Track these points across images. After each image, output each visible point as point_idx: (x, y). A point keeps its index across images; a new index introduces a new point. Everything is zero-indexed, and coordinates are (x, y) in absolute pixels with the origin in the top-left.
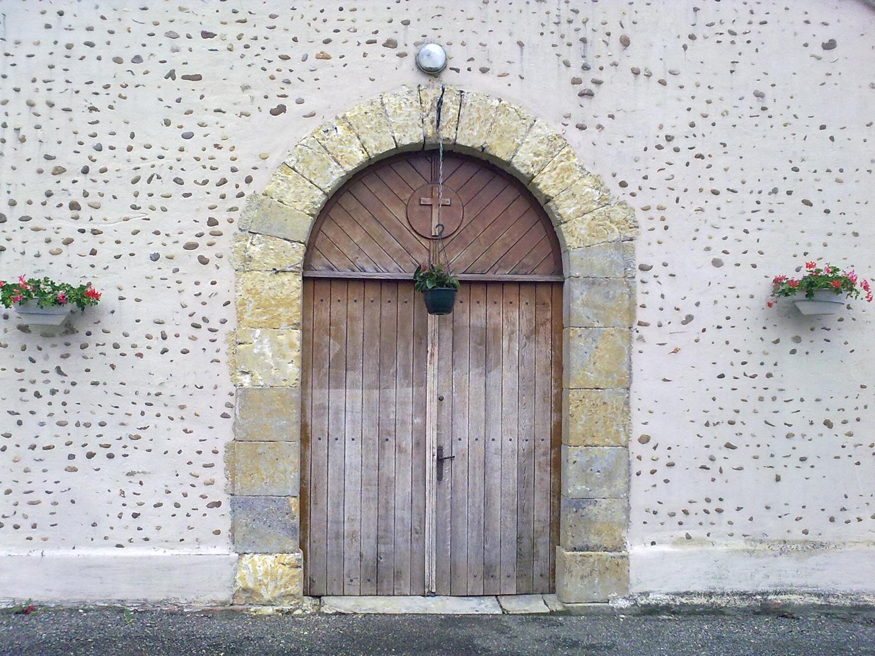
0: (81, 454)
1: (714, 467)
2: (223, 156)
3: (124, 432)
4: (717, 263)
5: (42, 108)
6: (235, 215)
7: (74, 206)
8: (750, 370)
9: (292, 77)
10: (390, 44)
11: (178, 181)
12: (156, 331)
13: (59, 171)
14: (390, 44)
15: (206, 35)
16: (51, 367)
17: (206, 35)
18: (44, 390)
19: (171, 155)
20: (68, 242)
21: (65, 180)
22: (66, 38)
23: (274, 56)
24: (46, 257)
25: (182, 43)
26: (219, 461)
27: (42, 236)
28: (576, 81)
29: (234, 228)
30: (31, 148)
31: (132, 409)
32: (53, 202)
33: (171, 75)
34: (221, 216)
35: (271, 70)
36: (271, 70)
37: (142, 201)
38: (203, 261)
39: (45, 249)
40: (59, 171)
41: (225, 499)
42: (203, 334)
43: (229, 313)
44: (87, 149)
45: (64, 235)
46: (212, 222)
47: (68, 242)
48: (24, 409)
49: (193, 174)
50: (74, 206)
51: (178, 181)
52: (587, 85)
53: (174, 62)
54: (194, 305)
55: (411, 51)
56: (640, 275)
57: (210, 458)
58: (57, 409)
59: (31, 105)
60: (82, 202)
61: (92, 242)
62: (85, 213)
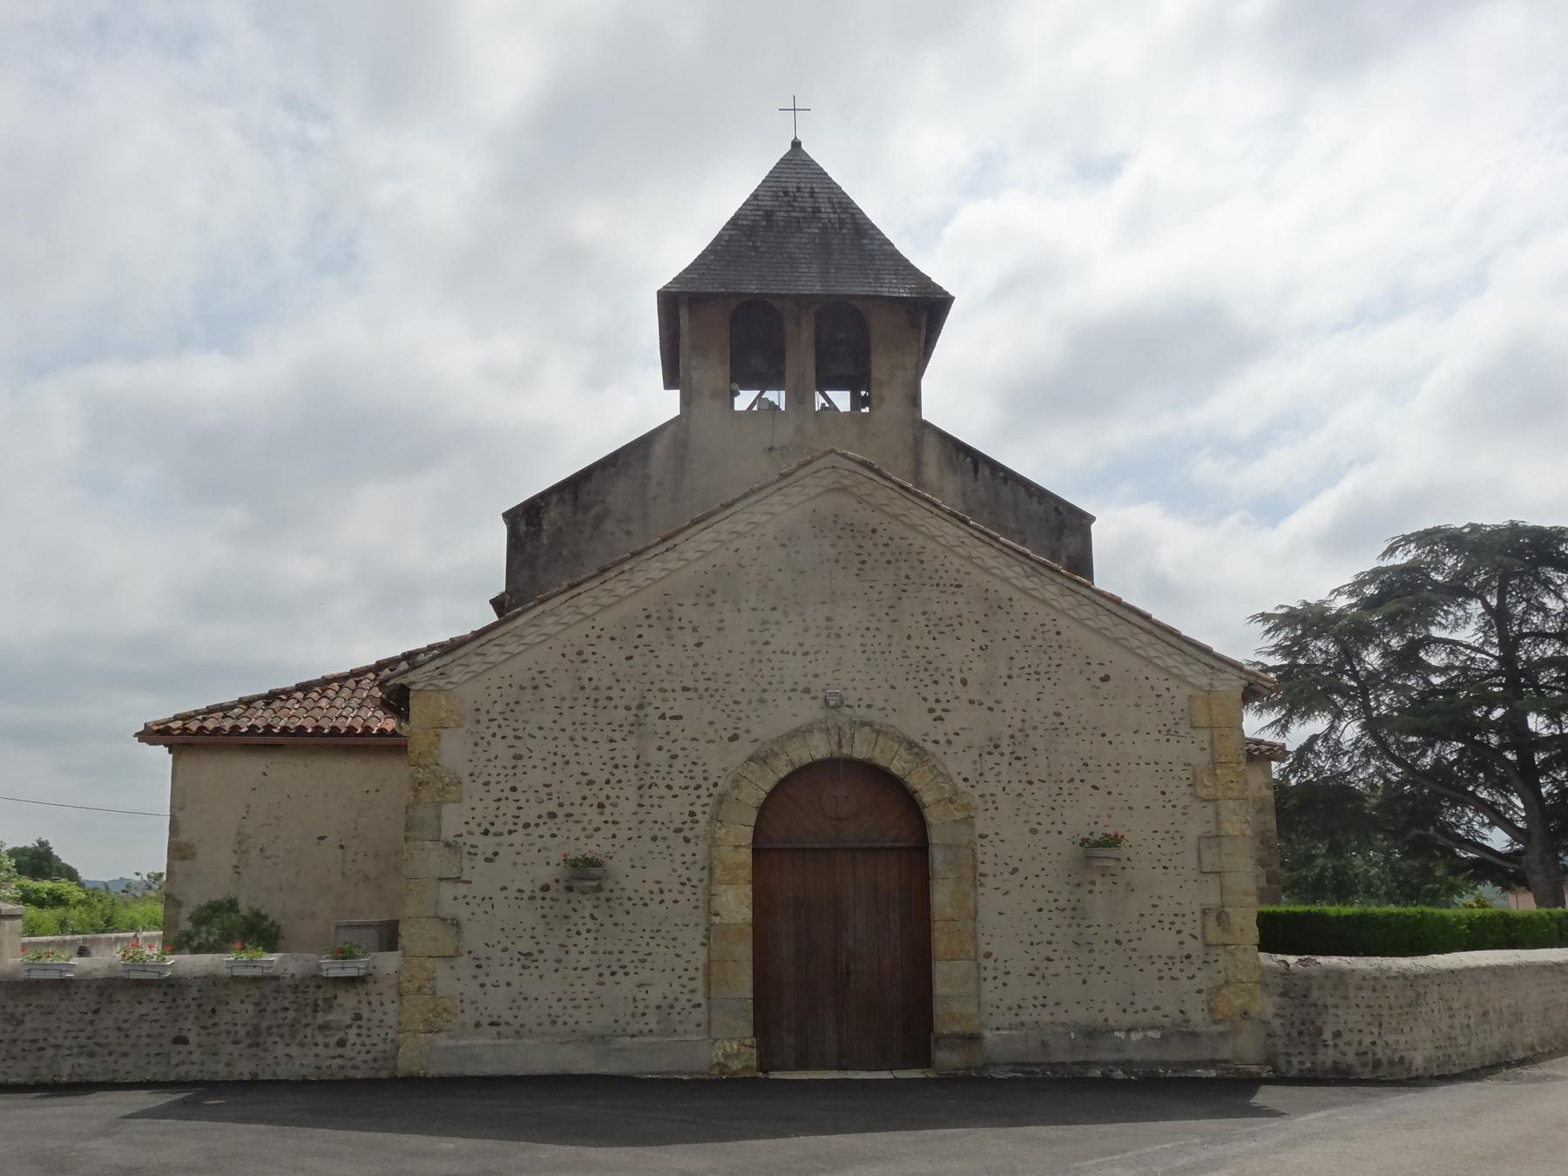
0: (607, 973)
1: (1038, 975)
2: (698, 770)
3: (635, 957)
4: (1034, 831)
5: (579, 741)
6: (707, 809)
7: (601, 806)
8: (1060, 904)
9: (742, 715)
10: (807, 691)
11: (669, 787)
12: (656, 888)
13: (591, 783)
14: (807, 691)
15: (685, 689)
16: (586, 914)
17: (685, 689)
18: (583, 929)
19: (664, 769)
20: (597, 829)
21: (595, 788)
22: (594, 695)
23: (728, 701)
24: (583, 840)
25: (669, 695)
26: (700, 975)
27: (580, 826)
28: (931, 711)
29: (707, 817)
30: (573, 768)
31: (639, 941)
32: (588, 802)
33: (663, 717)
34: (697, 809)
35: (728, 711)
36: (728, 711)
37: (646, 801)
38: (687, 840)
39: (582, 835)
40: (591, 783)
41: (703, 1002)
42: (688, 889)
43: (704, 875)
44: (609, 768)
45: (594, 825)
46: (692, 814)
47: (597, 829)
48: (569, 942)
49: (679, 781)
50: (601, 806)
51: (669, 787)
52: (938, 713)
53: (665, 708)
54: (681, 870)
55: (821, 695)
56: (980, 841)
57: (692, 973)
58: (591, 942)
59: (572, 739)
60: (607, 803)
61: (613, 829)
62: (608, 810)
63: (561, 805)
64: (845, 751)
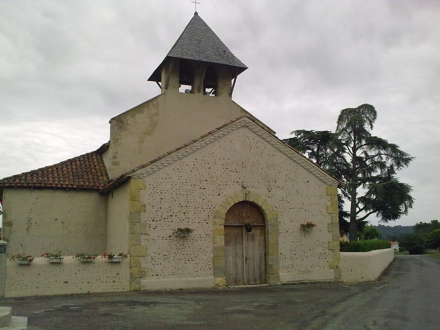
0: (187, 260)
1: (292, 258)
2: (210, 203)
3: (195, 256)
4: (291, 221)
5: (178, 195)
6: (212, 214)
7: (184, 213)
8: (298, 240)
9: (221, 189)
10: (237, 182)
11: (203, 208)
12: (199, 236)
13: (182, 206)
14: (237, 182)
15: (206, 181)
16: (181, 244)
17: (206, 181)
18: (180, 248)
19: (201, 203)
20: (184, 220)
21: (183, 208)
22: (182, 181)
23: (218, 184)
24: (180, 223)
25: (202, 182)
26: (211, 261)
27: (179, 219)
28: (268, 189)
29: (212, 217)
30: (177, 202)
31: (196, 251)
32: (181, 212)
33: (200, 188)
34: (210, 215)
35: (217, 187)
36: (217, 187)
37: (196, 212)
38: (207, 223)
39: (180, 221)
40: (182, 206)
41: (212, 268)
42: (208, 237)
43: (212, 233)
44: (186, 202)
45: (183, 219)
46: (209, 216)
47: (184, 220)
48: (177, 252)
49: (205, 207)
50: (184, 213)
51: (203, 208)
52: (270, 189)
53: (201, 186)
54: (206, 231)
55: (241, 183)
56: (279, 224)
57: (209, 260)
58: (183, 252)
59: (176, 194)
60: (186, 212)
61: (187, 220)
62: (186, 214)
63: (174, 213)
64: (247, 199)
